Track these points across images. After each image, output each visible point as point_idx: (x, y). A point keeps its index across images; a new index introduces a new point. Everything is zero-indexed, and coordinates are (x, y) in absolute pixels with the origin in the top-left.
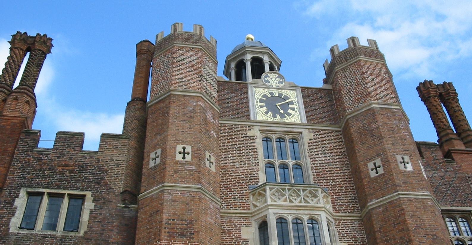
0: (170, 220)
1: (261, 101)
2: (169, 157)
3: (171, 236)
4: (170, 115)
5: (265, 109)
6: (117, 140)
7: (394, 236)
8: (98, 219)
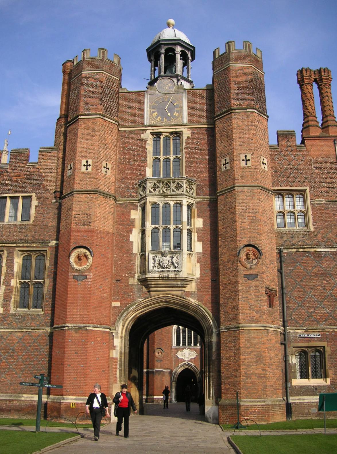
0: (77, 215)
2: (77, 170)
4: (79, 136)
5: (156, 113)
6: (50, 153)
7: (227, 217)
8: (40, 212)
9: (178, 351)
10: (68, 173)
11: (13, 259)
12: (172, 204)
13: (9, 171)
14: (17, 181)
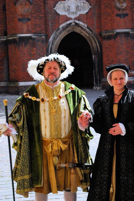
9: (57, 3)
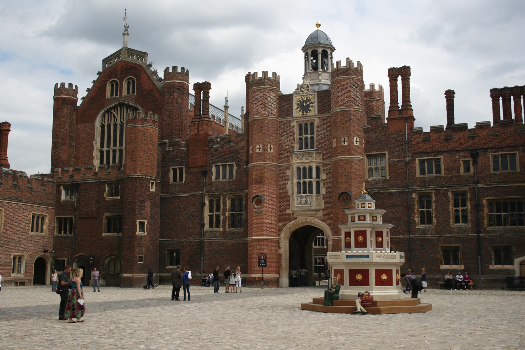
1: (298, 104)
3: (256, 183)
10: (251, 152)
11: (226, 201)
12: (307, 167)
13: (220, 149)
14: (225, 155)
